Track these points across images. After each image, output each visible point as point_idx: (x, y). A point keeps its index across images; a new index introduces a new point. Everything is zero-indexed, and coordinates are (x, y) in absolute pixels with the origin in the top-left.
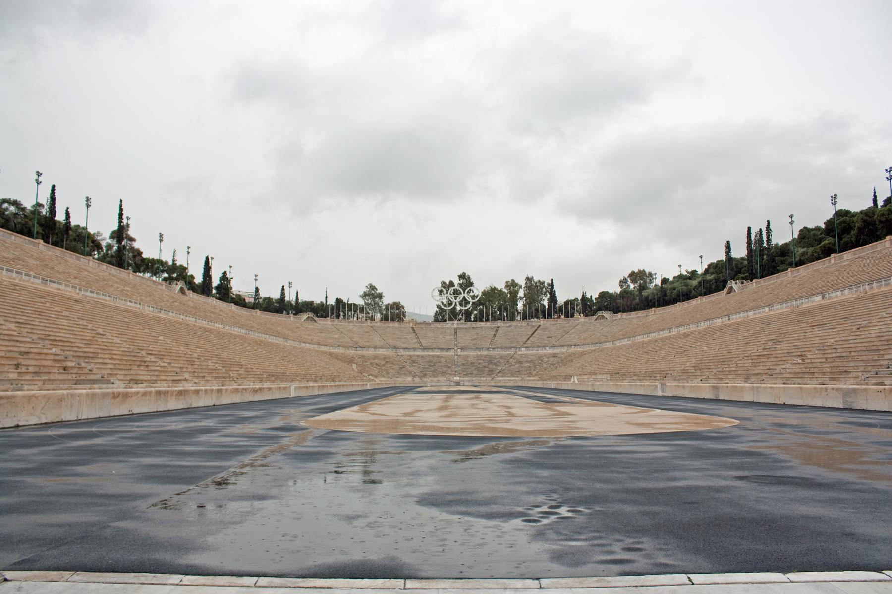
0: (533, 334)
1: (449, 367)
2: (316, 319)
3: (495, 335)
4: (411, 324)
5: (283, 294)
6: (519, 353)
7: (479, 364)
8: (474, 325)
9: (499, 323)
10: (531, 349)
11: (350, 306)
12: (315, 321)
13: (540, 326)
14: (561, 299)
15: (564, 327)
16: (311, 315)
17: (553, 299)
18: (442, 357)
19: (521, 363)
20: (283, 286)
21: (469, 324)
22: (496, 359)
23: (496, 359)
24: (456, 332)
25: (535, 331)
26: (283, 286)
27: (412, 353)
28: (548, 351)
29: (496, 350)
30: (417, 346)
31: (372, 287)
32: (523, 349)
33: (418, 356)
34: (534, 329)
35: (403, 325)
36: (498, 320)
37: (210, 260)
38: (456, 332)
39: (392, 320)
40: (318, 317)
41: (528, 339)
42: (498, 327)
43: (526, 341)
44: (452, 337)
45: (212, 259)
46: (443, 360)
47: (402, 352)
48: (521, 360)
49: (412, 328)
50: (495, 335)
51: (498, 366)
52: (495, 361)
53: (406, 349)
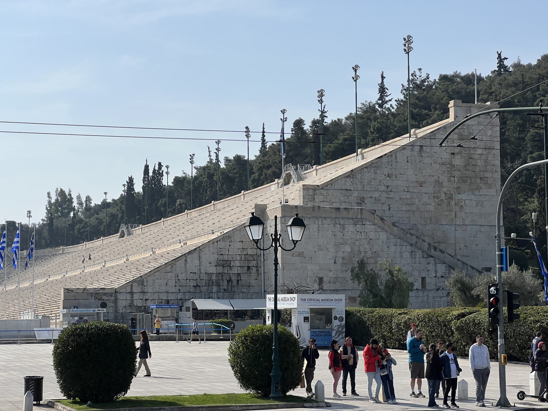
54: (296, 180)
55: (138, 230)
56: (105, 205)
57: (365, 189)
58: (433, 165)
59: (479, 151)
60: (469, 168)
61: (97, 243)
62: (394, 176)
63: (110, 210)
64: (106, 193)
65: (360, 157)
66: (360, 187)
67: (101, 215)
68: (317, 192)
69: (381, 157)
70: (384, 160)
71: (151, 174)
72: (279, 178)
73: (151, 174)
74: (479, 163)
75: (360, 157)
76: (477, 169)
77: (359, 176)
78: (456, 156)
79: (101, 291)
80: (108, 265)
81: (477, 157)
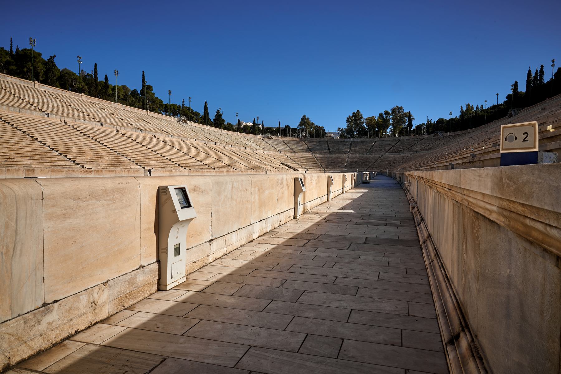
0: (395, 144)
2: (273, 137)
4: (327, 140)
5: (254, 123)
6: (384, 156)
7: (360, 162)
9: (377, 139)
10: (391, 153)
11: (292, 129)
12: (272, 138)
13: (400, 140)
14: (415, 124)
15: (414, 141)
16: (269, 135)
17: (410, 124)
18: (340, 158)
19: (383, 161)
20: (254, 119)
21: (359, 140)
22: (370, 159)
23: (370, 159)
24: (351, 144)
25: (396, 143)
26: (254, 119)
28: (401, 155)
31: (304, 118)
32: (387, 154)
34: (396, 142)
35: (322, 140)
36: (377, 137)
38: (351, 144)
39: (316, 137)
40: (274, 136)
41: (391, 148)
42: (376, 141)
43: (390, 149)
44: (349, 147)
48: (384, 160)
51: (370, 163)
52: (369, 160)
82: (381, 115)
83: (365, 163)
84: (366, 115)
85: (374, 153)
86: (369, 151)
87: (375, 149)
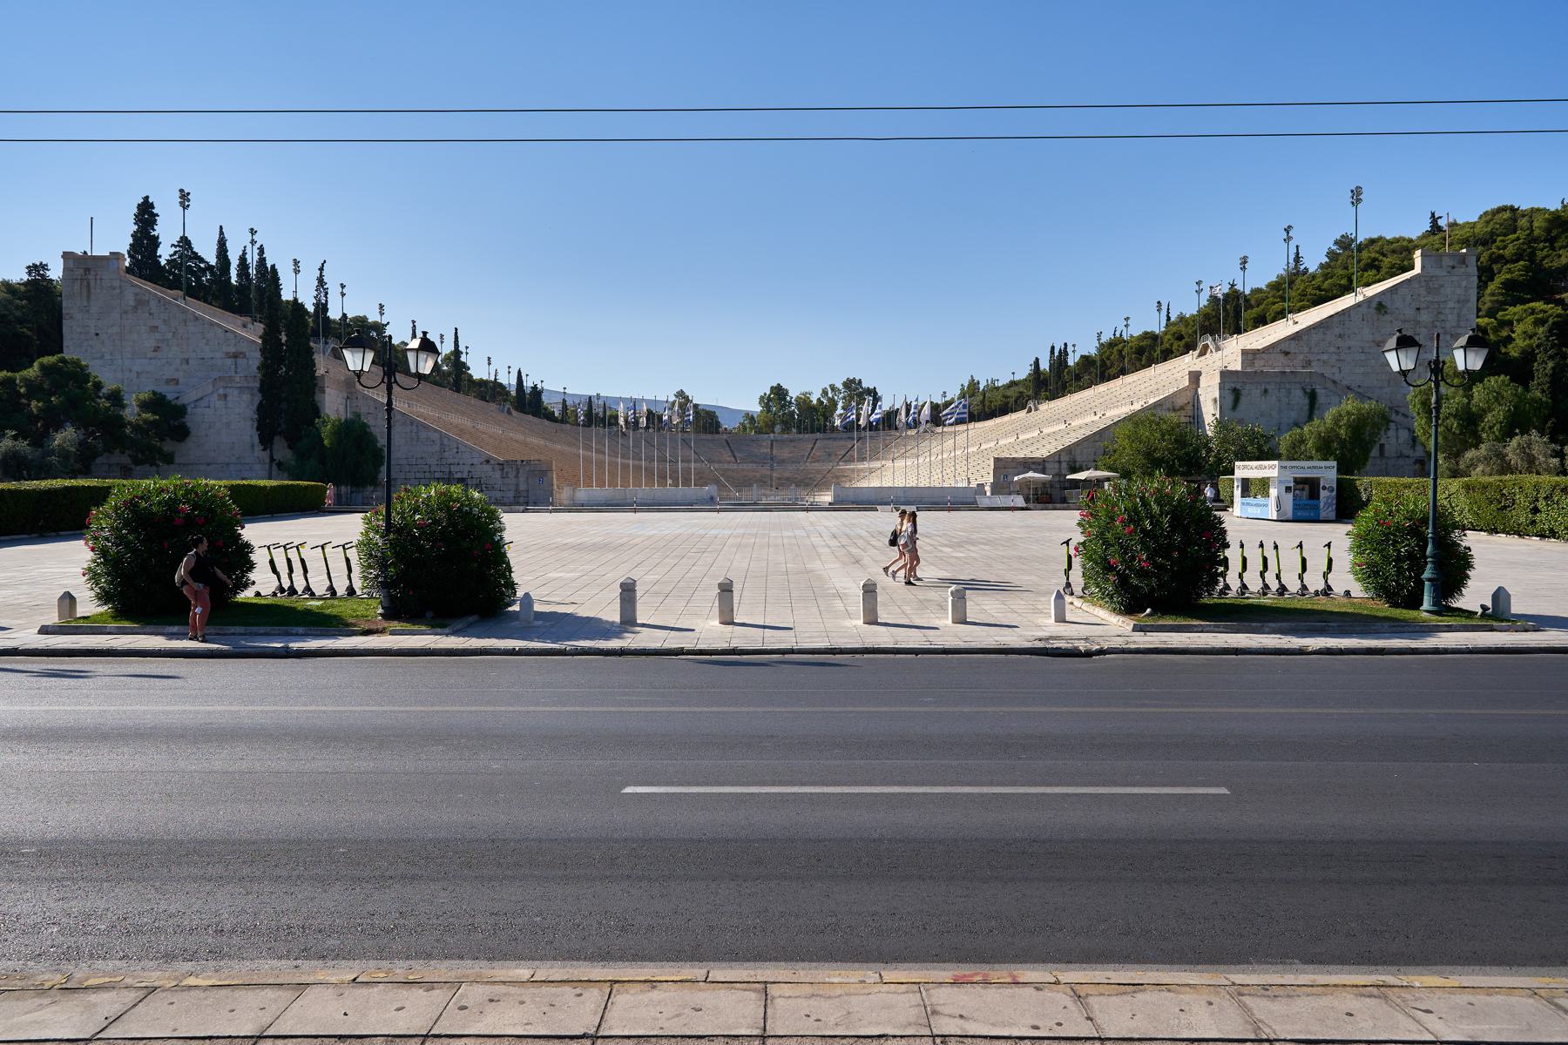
1: (765, 482)
3: (813, 448)
4: (725, 436)
8: (791, 436)
22: (812, 473)
23: (812, 473)
24: (772, 445)
27: (726, 466)
29: (813, 464)
30: (733, 460)
32: (841, 463)
33: (733, 471)
35: (717, 436)
37: (524, 378)
38: (772, 445)
43: (845, 455)
44: (769, 450)
45: (527, 375)
46: (758, 475)
47: (717, 466)
49: (727, 441)
50: (813, 448)
52: (812, 476)
53: (720, 462)
54: (1214, 350)
55: (1044, 407)
56: (1013, 384)
57: (1312, 350)
58: (1394, 322)
59: (1451, 305)
60: (1438, 324)
61: (1006, 418)
62: (1346, 336)
63: (1016, 388)
64: (1013, 373)
65: (1291, 322)
66: (1306, 349)
67: (1009, 393)
68: (1258, 356)
69: (1332, 316)
70: (1335, 319)
71: (1056, 353)
72: (1194, 350)
73: (1056, 353)
74: (1450, 317)
75: (1291, 322)
76: (1448, 325)
77: (1305, 338)
78: (1422, 312)
79: (1030, 460)
80: (1022, 437)
81: (1447, 311)
82: (825, 392)
83: (806, 481)
84: (794, 393)
85: (818, 461)
86: (808, 458)
87: (818, 454)
